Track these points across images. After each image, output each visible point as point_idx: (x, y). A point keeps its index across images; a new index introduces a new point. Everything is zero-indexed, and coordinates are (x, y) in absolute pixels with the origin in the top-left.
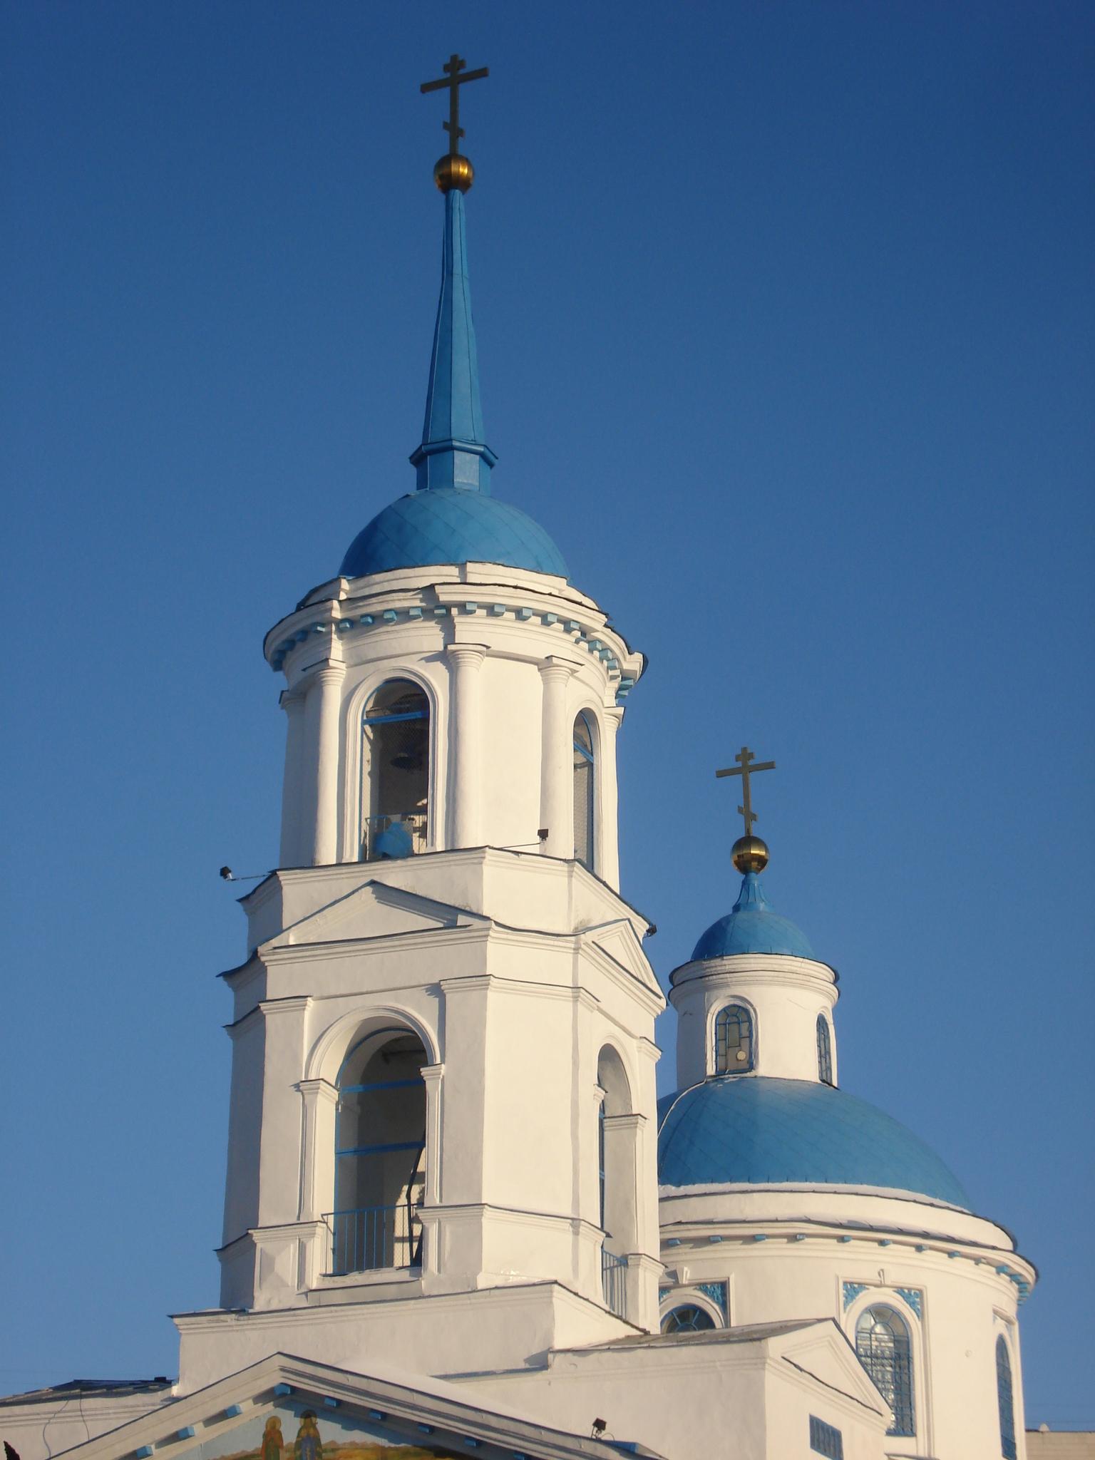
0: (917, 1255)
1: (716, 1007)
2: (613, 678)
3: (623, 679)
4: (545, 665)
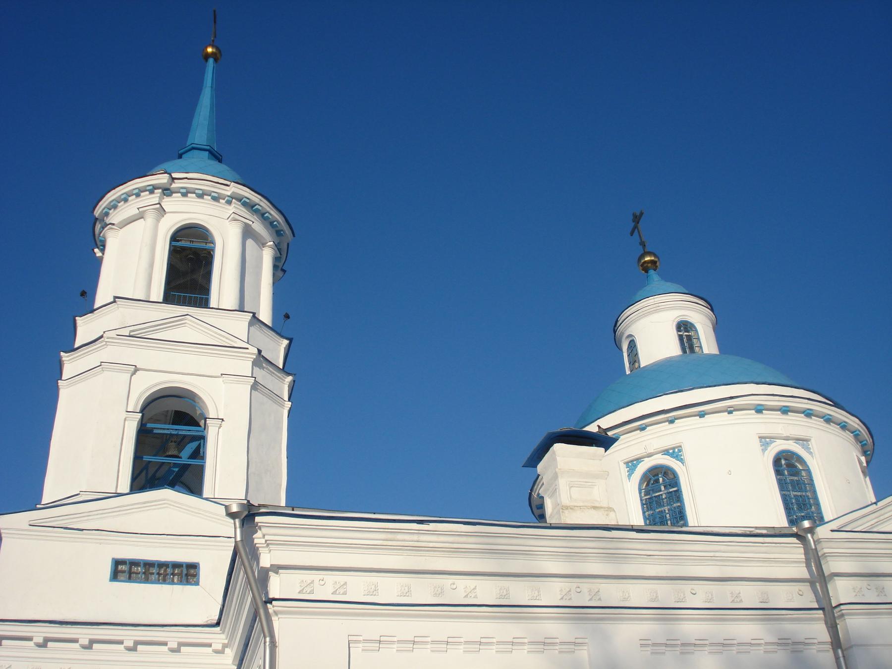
0: (672, 426)
1: (625, 347)
2: (229, 203)
3: (240, 200)
4: (141, 216)
